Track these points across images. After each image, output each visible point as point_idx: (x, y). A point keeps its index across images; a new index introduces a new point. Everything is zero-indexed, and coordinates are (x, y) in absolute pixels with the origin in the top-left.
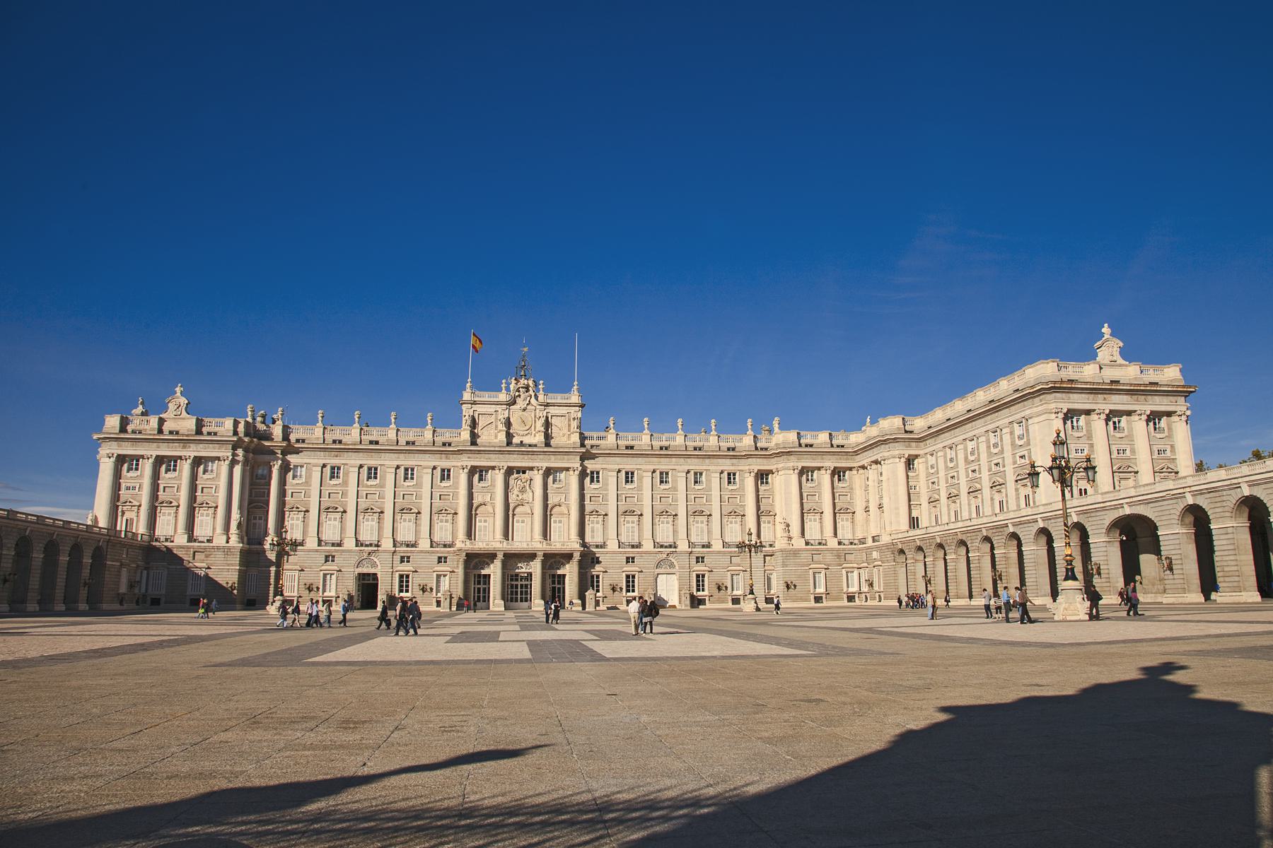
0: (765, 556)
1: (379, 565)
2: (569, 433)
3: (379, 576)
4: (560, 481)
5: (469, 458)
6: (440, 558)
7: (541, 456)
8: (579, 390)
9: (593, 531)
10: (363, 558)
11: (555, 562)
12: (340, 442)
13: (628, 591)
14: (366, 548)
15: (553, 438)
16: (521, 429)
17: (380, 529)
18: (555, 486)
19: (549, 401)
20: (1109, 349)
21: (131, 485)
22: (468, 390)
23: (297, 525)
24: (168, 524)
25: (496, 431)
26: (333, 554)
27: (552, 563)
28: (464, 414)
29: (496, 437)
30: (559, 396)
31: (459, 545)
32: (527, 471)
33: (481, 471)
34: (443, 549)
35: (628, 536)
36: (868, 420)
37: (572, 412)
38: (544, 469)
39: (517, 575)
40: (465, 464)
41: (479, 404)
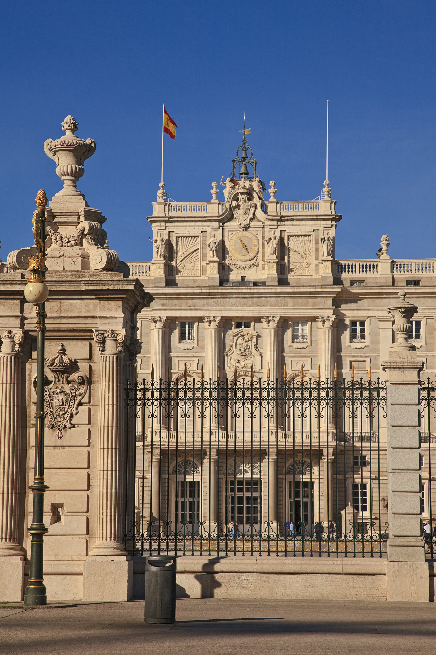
2: (316, 262)
4: (303, 337)
5: (163, 305)
7: (273, 301)
15: (291, 270)
16: (242, 258)
18: (296, 345)
19: (284, 213)
22: (160, 200)
25: (204, 263)
28: (154, 238)
29: (204, 272)
30: (300, 204)
32: (252, 324)
33: (183, 325)
37: (321, 228)
38: (277, 319)
39: (240, 483)
40: (157, 314)
41: (178, 221)
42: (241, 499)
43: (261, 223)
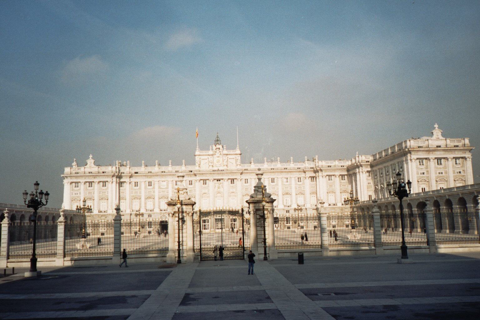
5: (199, 176)
8: (240, 149)
12: (151, 172)
20: (437, 133)
21: (76, 193)
30: (232, 151)
32: (221, 180)
36: (357, 153)
40: (197, 179)
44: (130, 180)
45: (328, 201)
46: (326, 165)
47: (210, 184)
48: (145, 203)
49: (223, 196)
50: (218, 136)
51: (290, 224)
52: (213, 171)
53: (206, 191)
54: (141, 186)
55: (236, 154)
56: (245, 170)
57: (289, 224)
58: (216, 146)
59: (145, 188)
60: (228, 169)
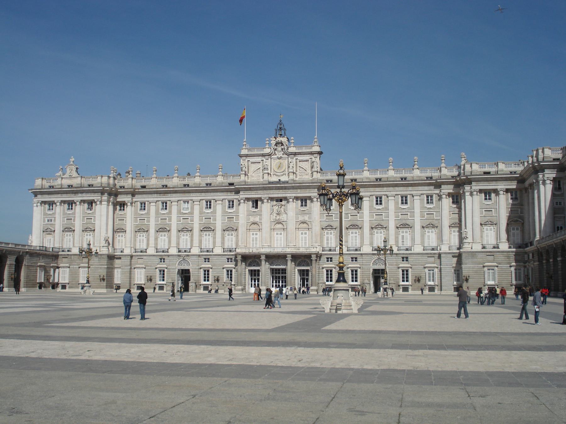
0: (452, 256)
1: (190, 263)
3: (191, 271)
5: (244, 193)
6: (228, 259)
9: (328, 240)
10: (181, 260)
11: (302, 261)
12: (166, 186)
13: (353, 281)
14: (182, 254)
17: (192, 241)
23: (143, 240)
24: (70, 241)
26: (164, 257)
27: (300, 262)
31: (238, 251)
34: (229, 253)
35: (352, 243)
40: (241, 196)
42: (279, 277)
43: (287, 156)
44: (132, 199)
45: (482, 241)
46: (479, 170)
47: (265, 207)
48: (156, 239)
49: (286, 229)
50: (281, 121)
51: (409, 283)
52: (270, 183)
53: (257, 219)
54: (149, 210)
55: (312, 153)
56: (327, 181)
57: (405, 283)
58: (276, 139)
59: (157, 212)
60: (297, 179)
